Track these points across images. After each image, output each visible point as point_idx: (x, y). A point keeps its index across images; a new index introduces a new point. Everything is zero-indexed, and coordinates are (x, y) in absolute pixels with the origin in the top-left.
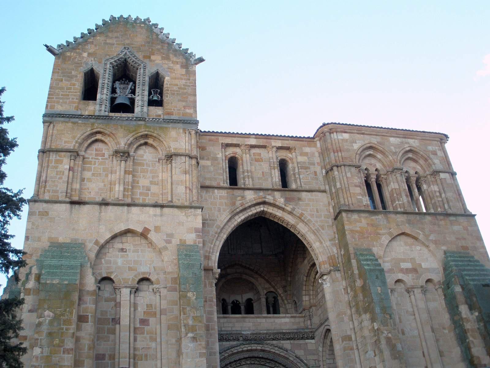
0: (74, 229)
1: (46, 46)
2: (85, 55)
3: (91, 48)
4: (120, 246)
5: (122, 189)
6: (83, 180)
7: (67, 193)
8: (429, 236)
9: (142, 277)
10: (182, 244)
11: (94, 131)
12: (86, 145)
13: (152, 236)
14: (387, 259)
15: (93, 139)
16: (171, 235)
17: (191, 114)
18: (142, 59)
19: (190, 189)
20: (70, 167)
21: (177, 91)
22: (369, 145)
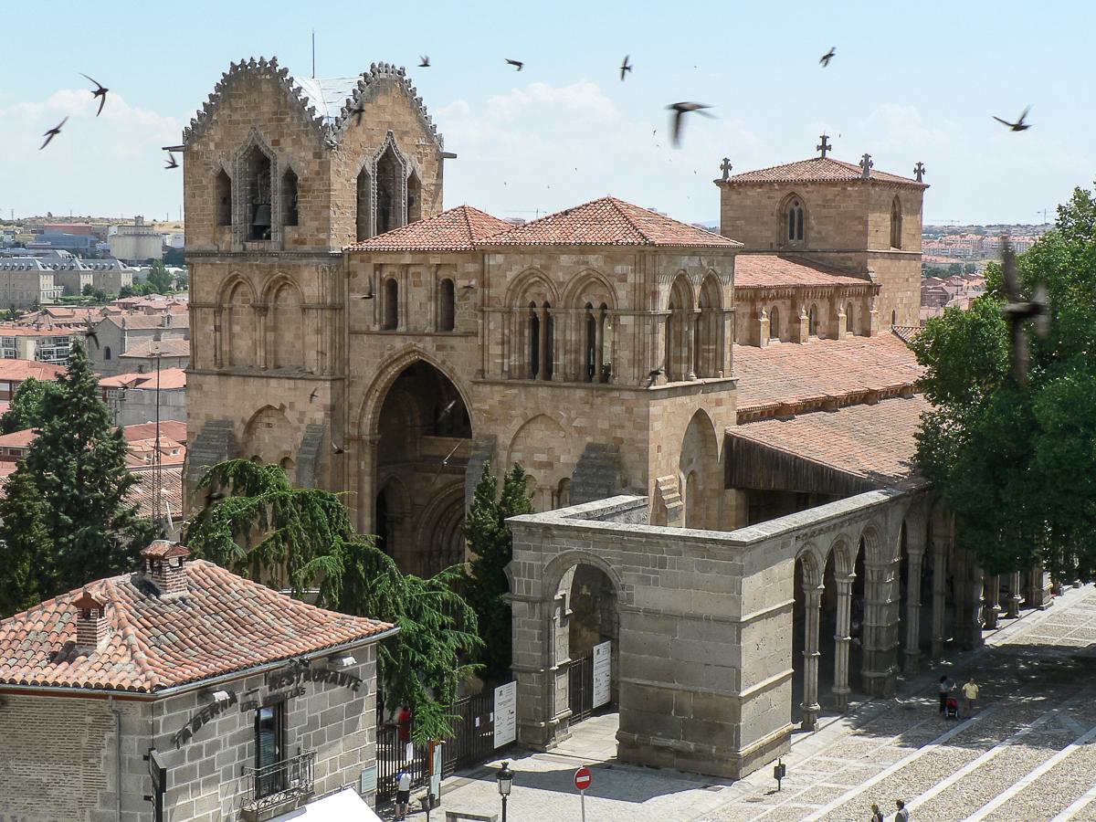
0: (224, 405)
1: (164, 149)
2: (212, 146)
3: (216, 133)
4: (266, 420)
5: (263, 354)
6: (232, 336)
7: (216, 360)
8: (573, 420)
9: (283, 456)
10: (312, 426)
11: (232, 274)
12: (230, 292)
13: (288, 413)
14: (521, 447)
15: (235, 283)
16: (303, 414)
17: (324, 241)
18: (271, 148)
19: (322, 353)
20: (215, 326)
21: (310, 202)
22: (527, 273)
